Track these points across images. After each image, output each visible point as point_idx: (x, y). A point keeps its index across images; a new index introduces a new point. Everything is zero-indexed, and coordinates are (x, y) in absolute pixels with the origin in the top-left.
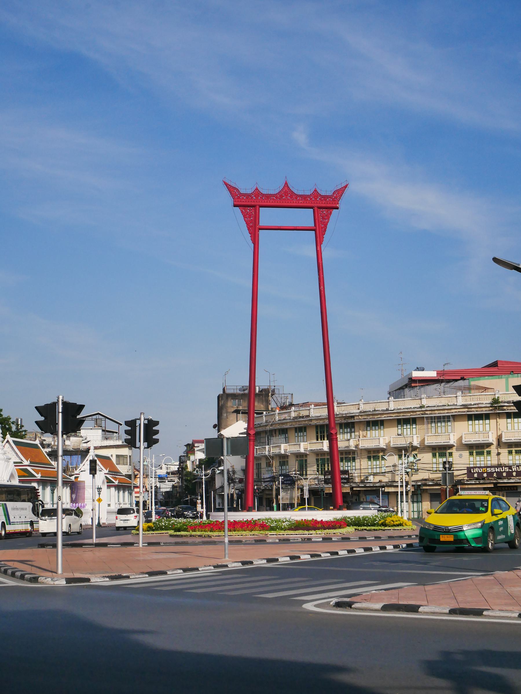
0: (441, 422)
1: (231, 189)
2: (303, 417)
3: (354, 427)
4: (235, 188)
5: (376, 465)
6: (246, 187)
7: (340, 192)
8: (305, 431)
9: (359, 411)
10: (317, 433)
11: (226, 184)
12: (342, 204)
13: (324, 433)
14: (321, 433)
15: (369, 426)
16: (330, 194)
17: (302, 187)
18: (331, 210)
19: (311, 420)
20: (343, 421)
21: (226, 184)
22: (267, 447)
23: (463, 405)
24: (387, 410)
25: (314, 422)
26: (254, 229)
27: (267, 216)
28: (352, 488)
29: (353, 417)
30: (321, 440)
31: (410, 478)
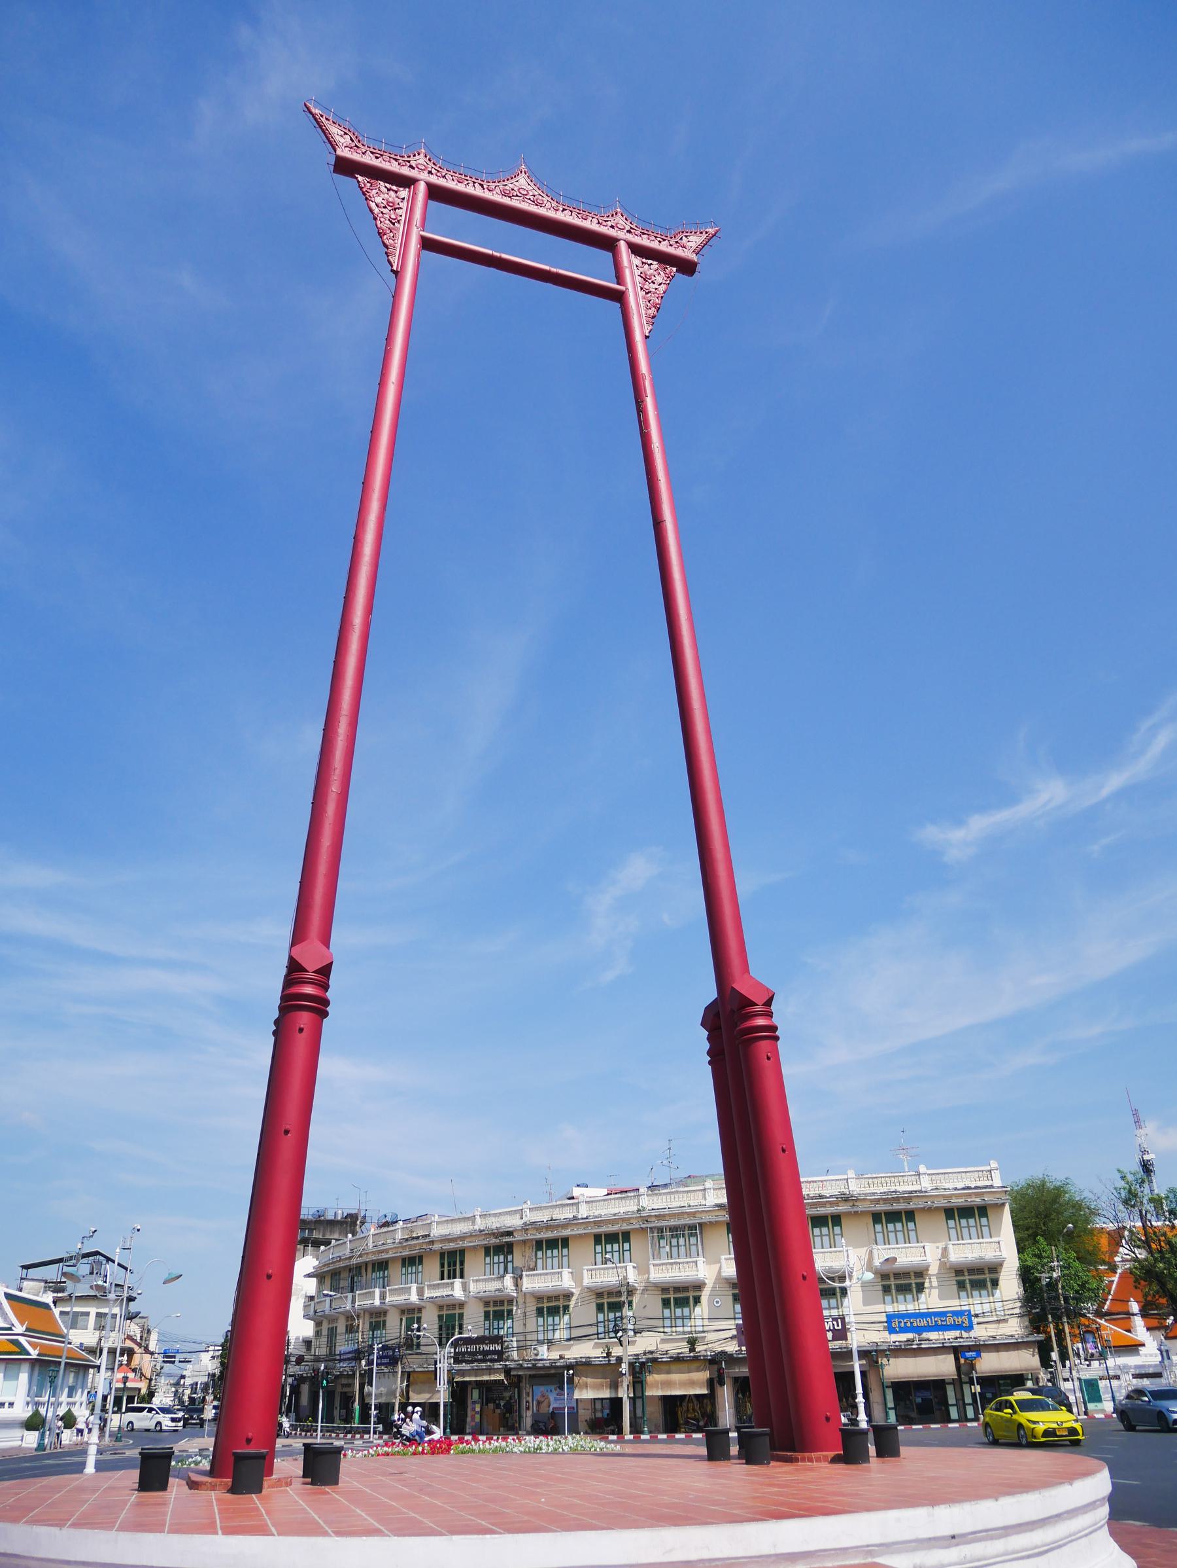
0: (678, 1237)
2: (417, 1238)
3: (511, 1252)
5: (554, 1325)
8: (421, 1263)
9: (521, 1222)
10: (442, 1266)
13: (455, 1265)
14: (449, 1265)
15: (541, 1249)
19: (432, 1242)
20: (493, 1241)
22: (377, 1291)
23: (717, 1205)
24: (575, 1218)
25: (437, 1247)
28: (507, 1371)
29: (509, 1234)
30: (449, 1278)
31: (625, 1351)
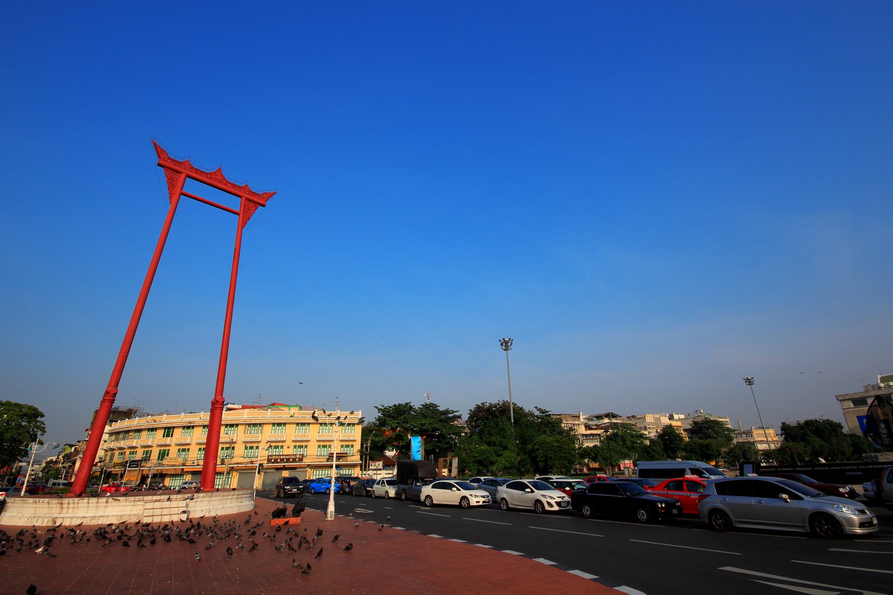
1: (160, 152)
4: (164, 151)
6: (177, 153)
11: (155, 144)
12: (268, 204)
17: (234, 177)
21: (155, 144)
26: (176, 192)
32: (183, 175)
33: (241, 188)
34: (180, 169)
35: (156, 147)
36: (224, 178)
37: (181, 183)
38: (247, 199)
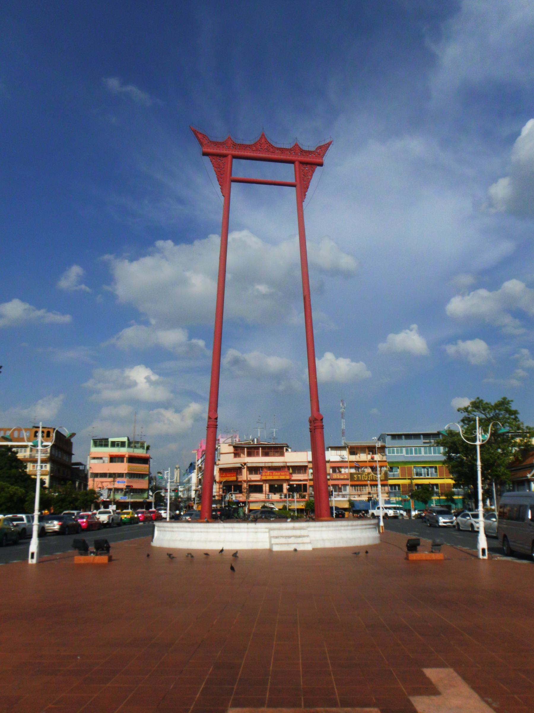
4: (204, 136)
7: (324, 148)
12: (326, 160)
16: (313, 149)
18: (314, 166)
26: (226, 180)
27: (241, 169)
32: (230, 157)
33: (290, 150)
34: (225, 152)
35: (195, 133)
36: (271, 145)
37: (229, 169)
38: (302, 163)
